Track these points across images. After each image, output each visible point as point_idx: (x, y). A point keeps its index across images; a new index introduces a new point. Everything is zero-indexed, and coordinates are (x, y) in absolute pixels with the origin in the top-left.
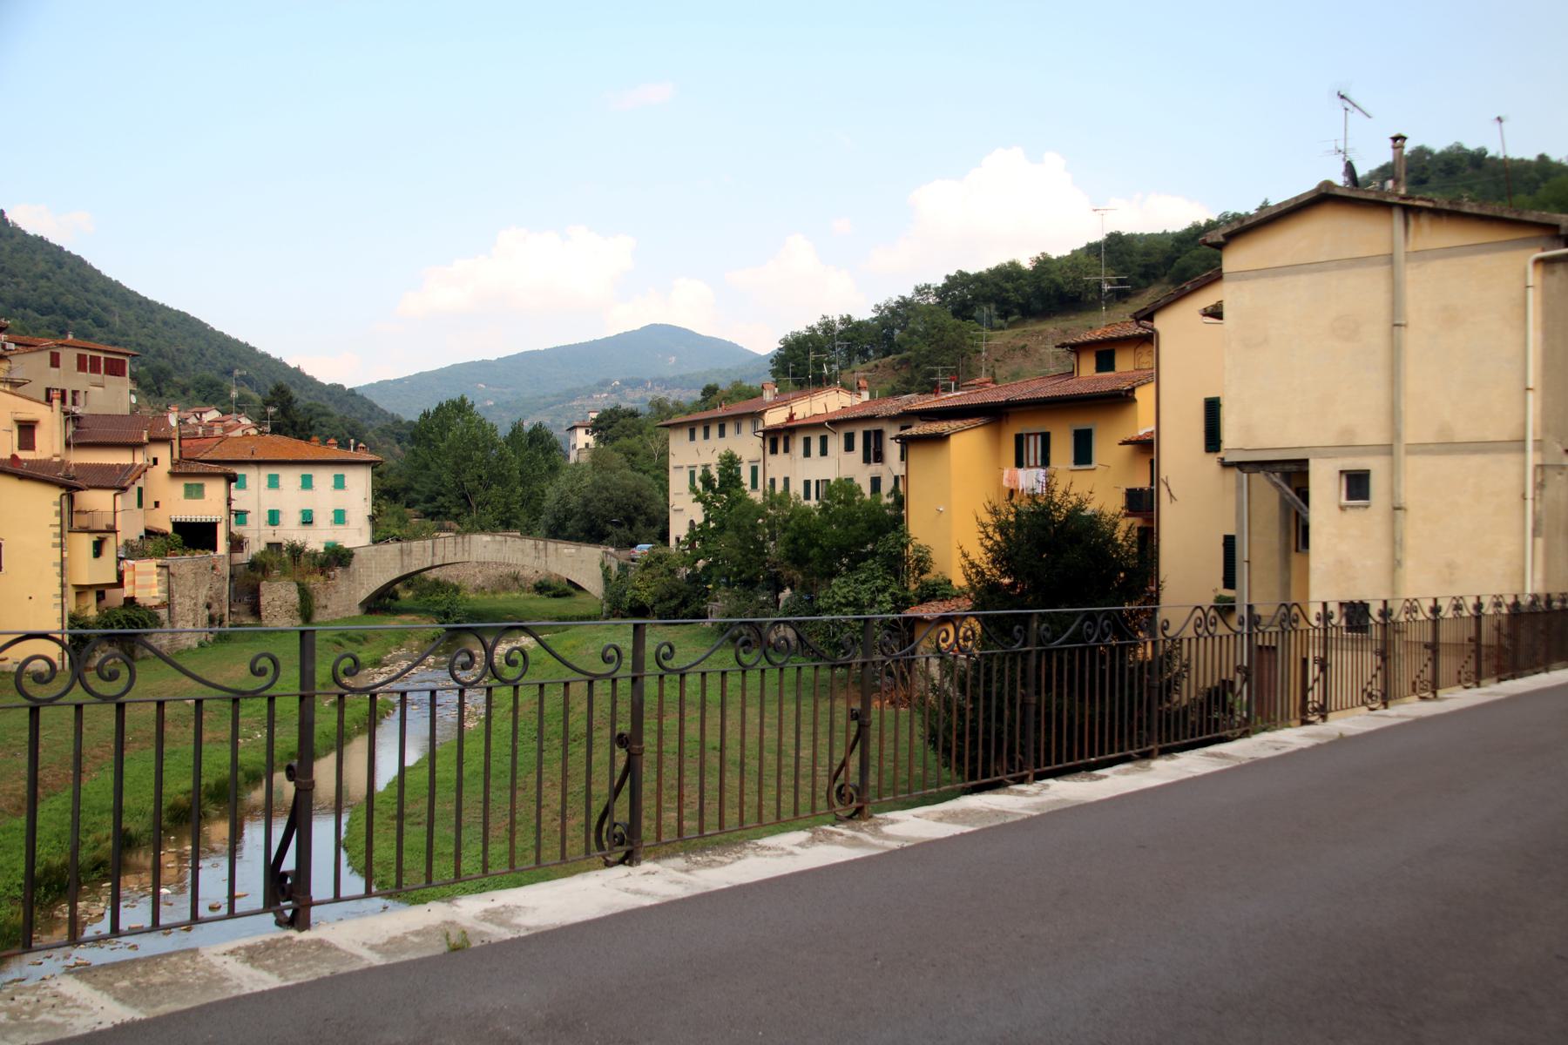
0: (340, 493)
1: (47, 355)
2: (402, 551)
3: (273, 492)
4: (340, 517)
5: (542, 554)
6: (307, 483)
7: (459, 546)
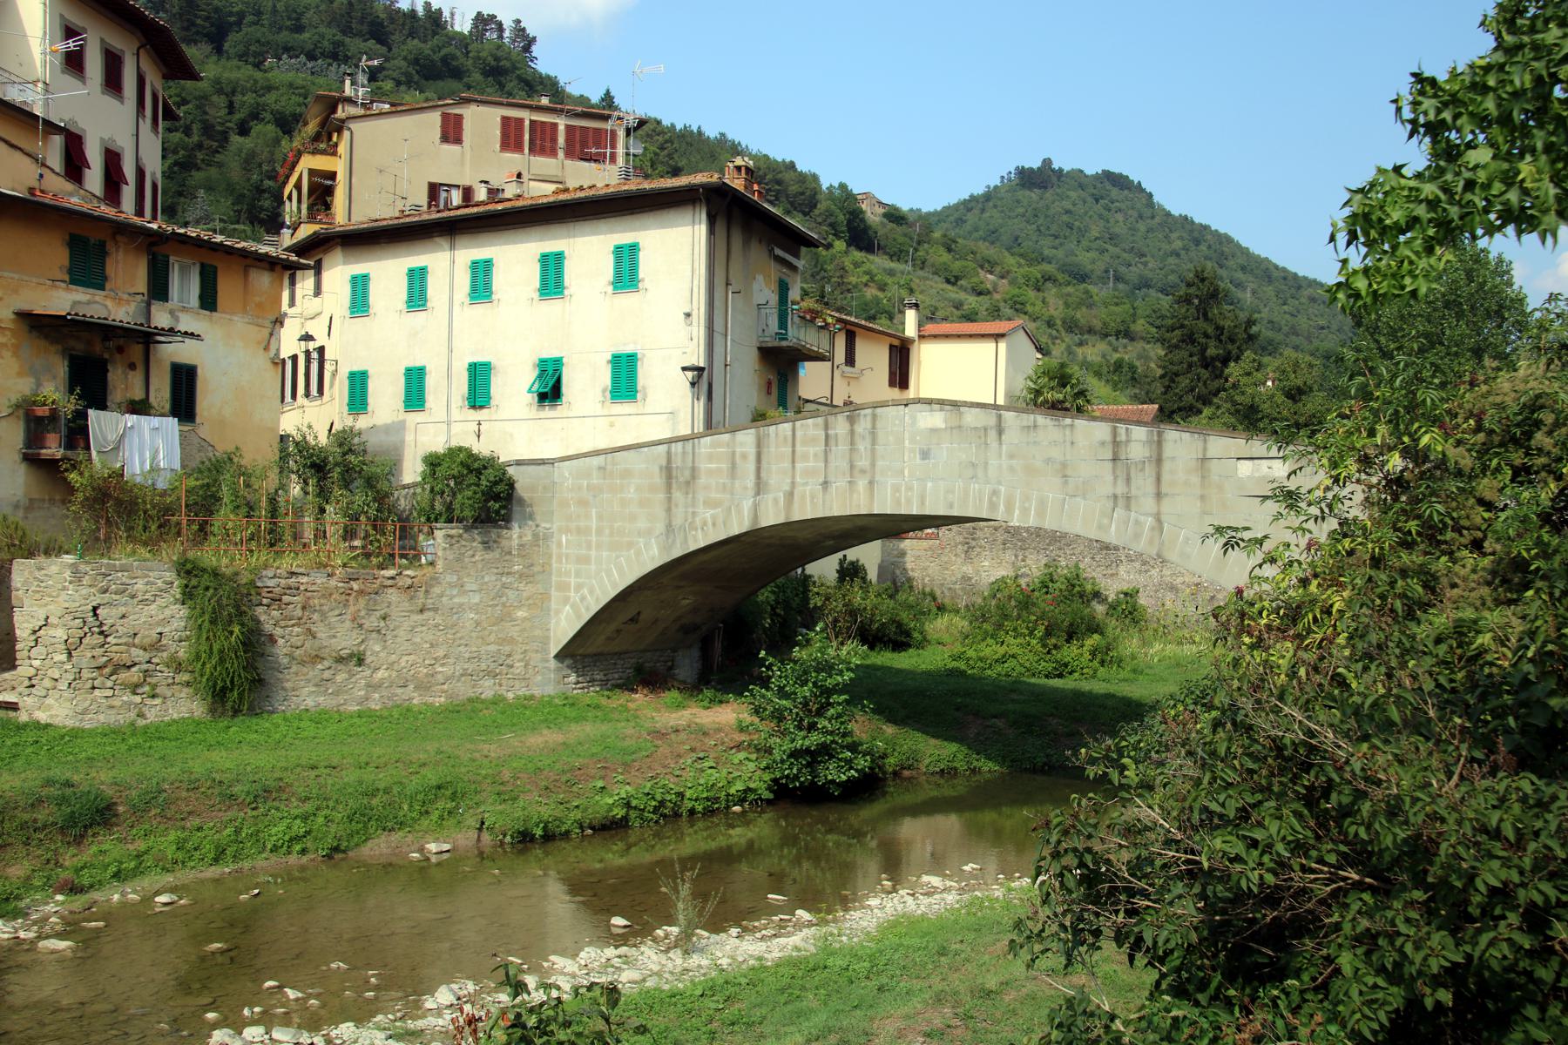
0: (627, 300)
1: (434, 119)
2: (668, 471)
3: (481, 309)
4: (624, 376)
5: (1143, 484)
6: (552, 277)
7: (841, 448)
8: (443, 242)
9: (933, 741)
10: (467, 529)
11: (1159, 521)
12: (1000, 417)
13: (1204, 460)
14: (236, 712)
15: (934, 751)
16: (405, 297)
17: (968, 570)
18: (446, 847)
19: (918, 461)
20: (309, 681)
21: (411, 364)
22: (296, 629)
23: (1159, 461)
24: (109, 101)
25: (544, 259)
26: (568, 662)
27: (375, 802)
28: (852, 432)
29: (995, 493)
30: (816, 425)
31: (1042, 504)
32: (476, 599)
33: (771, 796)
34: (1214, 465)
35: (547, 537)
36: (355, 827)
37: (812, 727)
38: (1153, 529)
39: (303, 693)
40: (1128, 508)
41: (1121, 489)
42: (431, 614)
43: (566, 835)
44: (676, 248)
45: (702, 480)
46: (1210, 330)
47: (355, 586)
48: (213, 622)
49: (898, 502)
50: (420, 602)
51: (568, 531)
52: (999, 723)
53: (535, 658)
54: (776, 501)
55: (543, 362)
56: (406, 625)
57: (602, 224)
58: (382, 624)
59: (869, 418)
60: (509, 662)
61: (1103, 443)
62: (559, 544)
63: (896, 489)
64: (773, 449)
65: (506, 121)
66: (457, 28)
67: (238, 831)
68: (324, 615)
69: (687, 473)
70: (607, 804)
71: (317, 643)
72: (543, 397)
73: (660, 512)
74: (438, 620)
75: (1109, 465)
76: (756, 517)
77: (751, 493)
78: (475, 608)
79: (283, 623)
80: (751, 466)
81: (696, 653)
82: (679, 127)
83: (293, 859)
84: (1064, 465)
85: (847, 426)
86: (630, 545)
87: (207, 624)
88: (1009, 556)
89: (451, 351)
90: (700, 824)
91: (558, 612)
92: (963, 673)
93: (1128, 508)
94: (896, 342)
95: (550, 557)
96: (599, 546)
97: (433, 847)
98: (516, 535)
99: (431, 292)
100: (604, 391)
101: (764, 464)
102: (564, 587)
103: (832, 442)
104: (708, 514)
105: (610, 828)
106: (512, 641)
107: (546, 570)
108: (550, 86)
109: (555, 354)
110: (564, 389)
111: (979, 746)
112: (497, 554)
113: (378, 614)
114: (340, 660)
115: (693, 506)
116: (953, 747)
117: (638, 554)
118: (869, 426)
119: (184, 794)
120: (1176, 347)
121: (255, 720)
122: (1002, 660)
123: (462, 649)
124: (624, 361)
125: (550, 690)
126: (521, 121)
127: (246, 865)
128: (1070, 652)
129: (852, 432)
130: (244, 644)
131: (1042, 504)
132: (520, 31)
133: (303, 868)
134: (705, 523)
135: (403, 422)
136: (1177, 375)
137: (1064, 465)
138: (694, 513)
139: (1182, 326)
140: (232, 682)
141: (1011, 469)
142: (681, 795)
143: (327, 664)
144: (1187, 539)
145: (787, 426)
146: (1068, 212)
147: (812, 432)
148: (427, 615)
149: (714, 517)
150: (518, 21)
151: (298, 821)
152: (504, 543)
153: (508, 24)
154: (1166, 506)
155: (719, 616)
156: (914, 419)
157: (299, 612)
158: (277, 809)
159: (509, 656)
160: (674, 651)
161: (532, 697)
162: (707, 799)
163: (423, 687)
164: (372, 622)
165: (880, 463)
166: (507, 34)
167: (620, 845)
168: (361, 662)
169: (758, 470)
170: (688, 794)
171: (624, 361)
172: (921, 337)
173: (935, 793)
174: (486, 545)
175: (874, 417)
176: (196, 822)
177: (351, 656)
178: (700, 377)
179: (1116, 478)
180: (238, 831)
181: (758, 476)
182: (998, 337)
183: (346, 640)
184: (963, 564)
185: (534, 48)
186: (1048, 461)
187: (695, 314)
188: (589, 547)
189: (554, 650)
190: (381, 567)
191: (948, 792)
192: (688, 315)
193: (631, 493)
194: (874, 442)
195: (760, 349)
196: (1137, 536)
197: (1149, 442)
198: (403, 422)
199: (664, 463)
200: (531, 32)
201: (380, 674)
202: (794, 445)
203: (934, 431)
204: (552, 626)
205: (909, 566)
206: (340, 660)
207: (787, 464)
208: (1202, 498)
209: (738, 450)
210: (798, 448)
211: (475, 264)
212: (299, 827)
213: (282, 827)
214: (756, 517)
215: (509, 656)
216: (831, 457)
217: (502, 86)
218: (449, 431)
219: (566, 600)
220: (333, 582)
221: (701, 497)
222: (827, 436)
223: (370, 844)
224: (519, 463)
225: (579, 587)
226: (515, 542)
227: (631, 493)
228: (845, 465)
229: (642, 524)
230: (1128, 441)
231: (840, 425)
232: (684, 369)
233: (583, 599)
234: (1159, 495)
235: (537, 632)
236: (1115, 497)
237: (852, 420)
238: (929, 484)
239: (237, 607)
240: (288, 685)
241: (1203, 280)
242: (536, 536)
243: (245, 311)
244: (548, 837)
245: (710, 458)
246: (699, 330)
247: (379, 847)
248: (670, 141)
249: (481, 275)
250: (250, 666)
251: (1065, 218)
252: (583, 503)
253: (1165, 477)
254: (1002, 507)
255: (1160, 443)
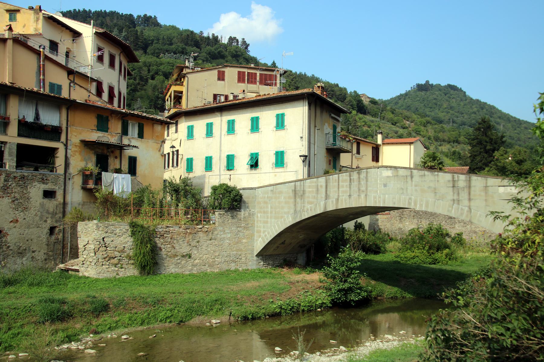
0: (281, 133)
1: (215, 72)
2: (295, 191)
3: (230, 137)
4: (280, 159)
5: (464, 195)
6: (255, 125)
8: (218, 114)
9: (389, 287)
10: (226, 212)
11: (470, 209)
12: (412, 172)
13: (486, 187)
14: (149, 274)
15: (389, 290)
16: (205, 132)
17: (401, 226)
18: (218, 321)
19: (383, 188)
20: (173, 263)
21: (207, 156)
22: (169, 246)
23: (470, 187)
24: (111, 71)
25: (252, 119)
26: (260, 257)
27: (194, 305)
28: (359, 178)
29: (410, 199)
30: (346, 175)
31: (427, 203)
32: (229, 236)
33: (331, 305)
34: (490, 189)
35: (253, 215)
36: (188, 314)
37: (346, 281)
38: (468, 211)
39: (170, 267)
40: (458, 204)
41: (456, 197)
42: (214, 241)
43: (259, 318)
44: (298, 115)
45: (307, 195)
46: (488, 140)
47: (188, 231)
48: (141, 243)
49: (376, 202)
50: (210, 236)
51: (260, 212)
52: (413, 280)
53: (249, 256)
54: (332, 201)
55: (252, 154)
56: (205, 244)
57: (272, 107)
58: (197, 244)
59: (365, 173)
60: (240, 257)
61: (449, 181)
62: (258, 217)
63: (375, 197)
64: (331, 184)
65: (239, 72)
66: (223, 42)
67: (149, 314)
68: (178, 241)
69: (302, 192)
70: (273, 308)
71: (175, 250)
72: (252, 166)
73: (292, 206)
74: (216, 243)
75: (451, 189)
76: (325, 208)
77: (324, 199)
78: (229, 239)
79: (164, 244)
80: (324, 190)
81: (305, 254)
82: (298, 73)
83: (167, 324)
84: (435, 189)
85: (357, 175)
86: (282, 217)
87: (139, 244)
88: (415, 221)
89: (221, 151)
90: (306, 315)
91: (257, 240)
92: (399, 262)
93: (458, 204)
94: (374, 146)
95: (254, 221)
96: (271, 218)
97: (214, 321)
98: (242, 214)
99: (214, 131)
100: (273, 164)
101: (328, 189)
102: (259, 232)
103: (352, 181)
104: (308, 206)
105: (275, 316)
106: (241, 250)
107: (253, 226)
108: (254, 60)
109: (256, 151)
110: (259, 164)
111: (405, 288)
112: (236, 220)
113: (196, 241)
114: (183, 256)
115: (304, 203)
116: (396, 289)
117: (285, 220)
118: (365, 175)
119: (131, 301)
120: (475, 146)
121: (155, 277)
122: (413, 258)
123: (224, 253)
124: (280, 154)
125: (254, 267)
126: (244, 72)
127: (151, 326)
128: (438, 255)
129: (359, 178)
130: (151, 250)
131: (427, 203)
132: (244, 42)
133: (170, 328)
134: (308, 210)
135: (205, 175)
136: (476, 156)
137: (435, 189)
138: (304, 206)
139: (477, 139)
140: (147, 263)
141: (416, 190)
142: (299, 304)
143: (179, 257)
144: (480, 215)
145: (336, 176)
146: (435, 99)
147: (345, 178)
148: (212, 241)
149: (311, 207)
150: (244, 39)
151: (169, 311)
152: (239, 216)
153: (240, 40)
154: (472, 203)
155: (313, 242)
156: (381, 173)
157: (169, 240)
158: (162, 307)
159: (240, 255)
160: (297, 254)
161: (248, 270)
162: (309, 306)
163: (211, 266)
164: (194, 243)
165: (369, 189)
166: (240, 43)
167: (279, 322)
168: (190, 257)
169: (326, 191)
170: (302, 304)
171: (280, 154)
172: (383, 144)
173: (389, 305)
174: (233, 217)
175: (367, 172)
176: (135, 311)
177: (187, 255)
178: (306, 159)
179: (454, 193)
180: (149, 314)
181: (326, 193)
182: (411, 143)
183: (185, 250)
184: (399, 224)
185: (249, 48)
186: (429, 187)
187: (304, 137)
188: (268, 218)
189: (256, 254)
190: (197, 225)
191: (394, 305)
192: (302, 138)
193: (282, 199)
194: (367, 181)
195: (327, 149)
196: (462, 214)
197: (466, 180)
198: (205, 175)
199: (293, 189)
200: (248, 42)
201: (197, 261)
202: (339, 182)
203: (388, 177)
204: (255, 245)
205: (380, 224)
206: (183, 256)
207: (336, 189)
208: (486, 200)
209: (319, 184)
210: (340, 184)
211: (229, 121)
212: (169, 314)
213: (163, 313)
214: (325, 208)
215: (240, 255)
216: (352, 187)
217: (238, 61)
218: (220, 178)
219: (260, 236)
220: (181, 230)
221: (306, 200)
222: (350, 179)
223: (193, 320)
224: (244, 189)
225: (264, 232)
226: (242, 216)
227: (282, 199)
228: (357, 189)
229: (286, 210)
230: (458, 180)
231: (355, 175)
232: (300, 156)
233: (266, 236)
234: (470, 200)
235: (250, 247)
236: (454, 200)
237: (359, 174)
238: (387, 196)
239: (149, 238)
240: (166, 265)
241: (485, 122)
242: (249, 214)
243: (153, 138)
244: (253, 319)
245: (310, 187)
246: (305, 143)
247: (196, 321)
248: (295, 78)
249: (231, 125)
250: (153, 258)
251: (434, 101)
252: (266, 203)
253: (472, 193)
254: (413, 204)
255: (470, 181)
